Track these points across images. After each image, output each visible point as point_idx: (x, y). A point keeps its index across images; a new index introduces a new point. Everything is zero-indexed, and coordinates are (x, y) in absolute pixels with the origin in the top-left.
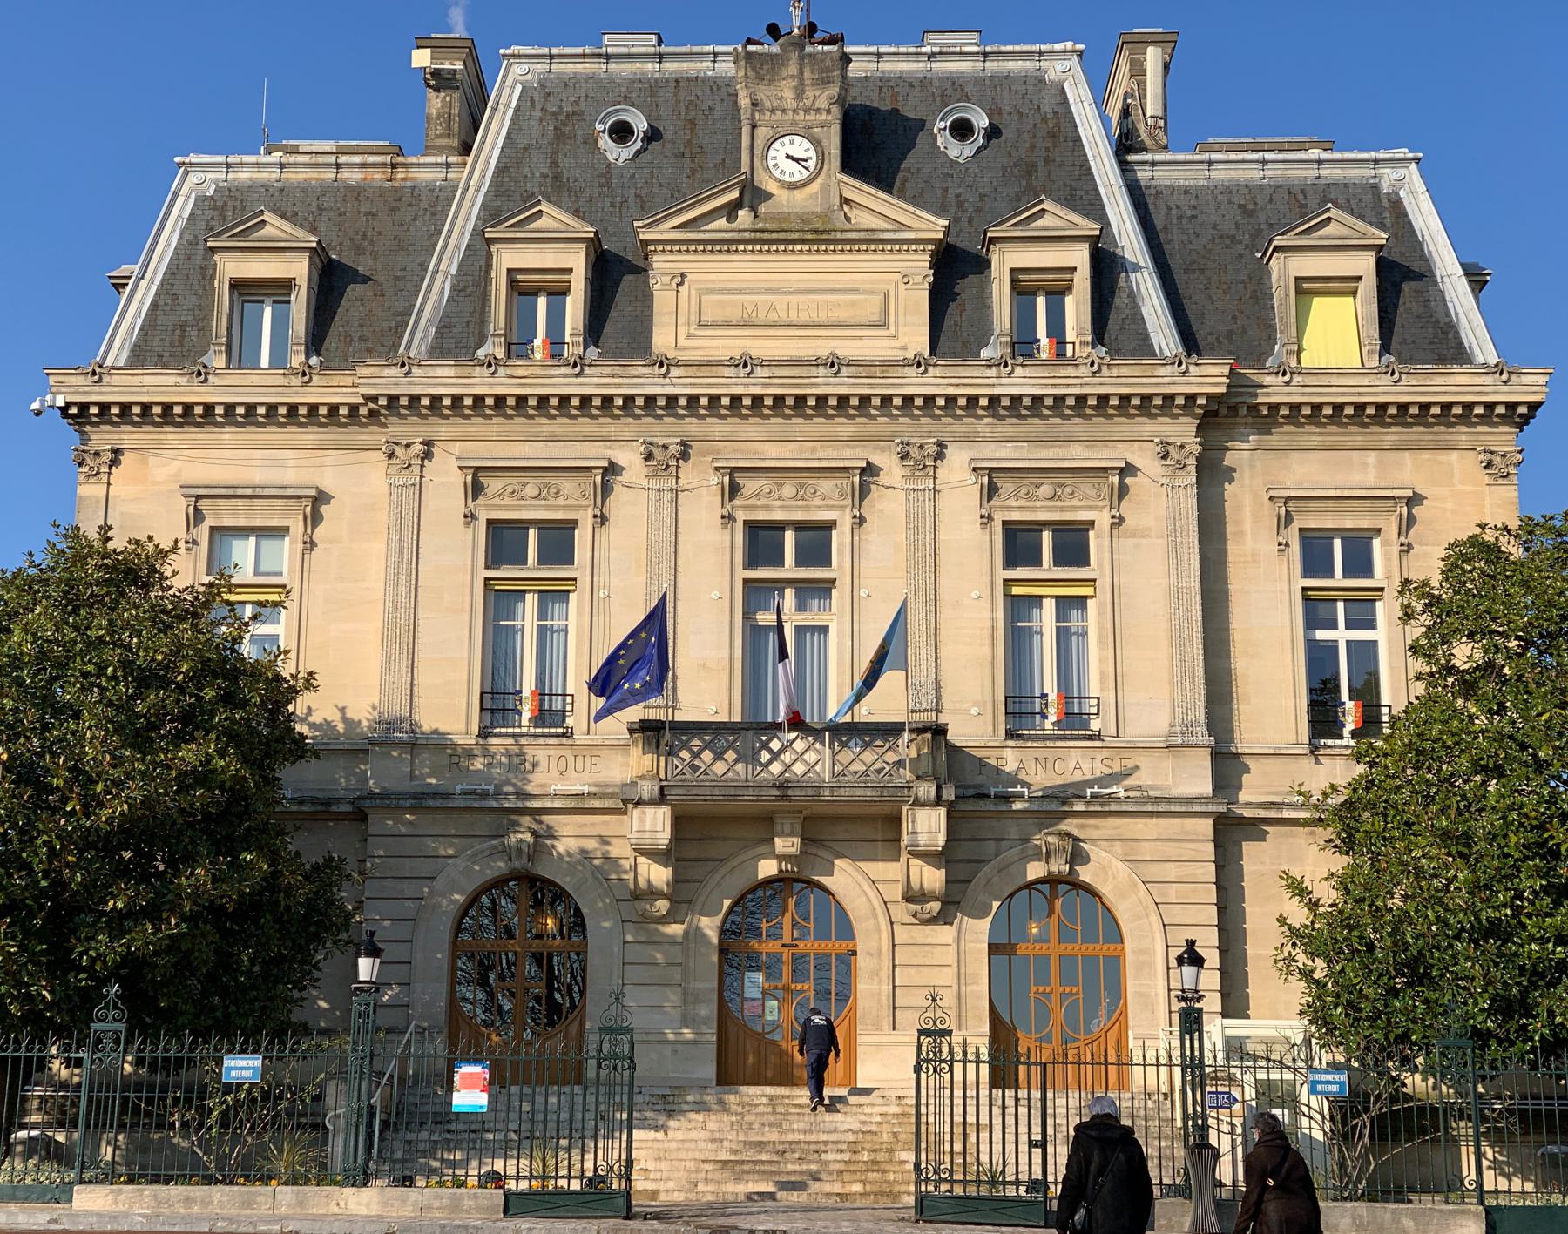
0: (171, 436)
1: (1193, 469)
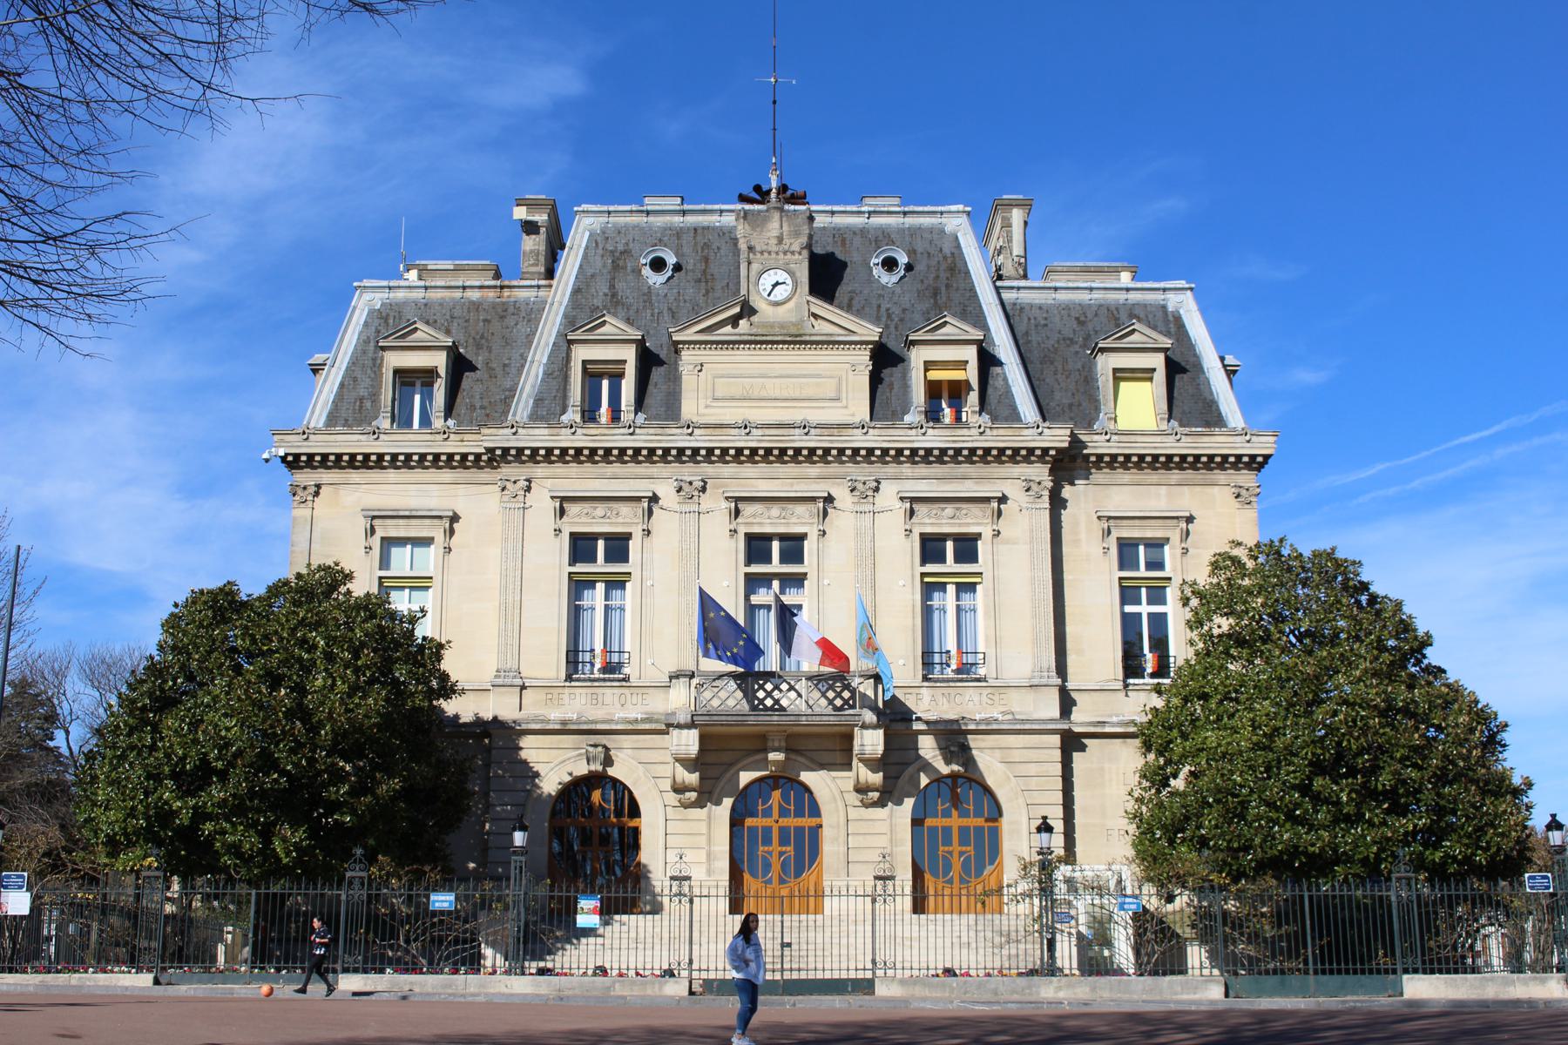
0: (355, 476)
1: (1046, 499)
